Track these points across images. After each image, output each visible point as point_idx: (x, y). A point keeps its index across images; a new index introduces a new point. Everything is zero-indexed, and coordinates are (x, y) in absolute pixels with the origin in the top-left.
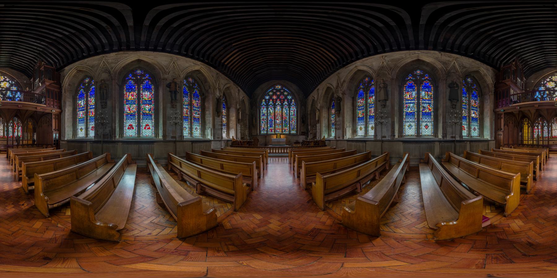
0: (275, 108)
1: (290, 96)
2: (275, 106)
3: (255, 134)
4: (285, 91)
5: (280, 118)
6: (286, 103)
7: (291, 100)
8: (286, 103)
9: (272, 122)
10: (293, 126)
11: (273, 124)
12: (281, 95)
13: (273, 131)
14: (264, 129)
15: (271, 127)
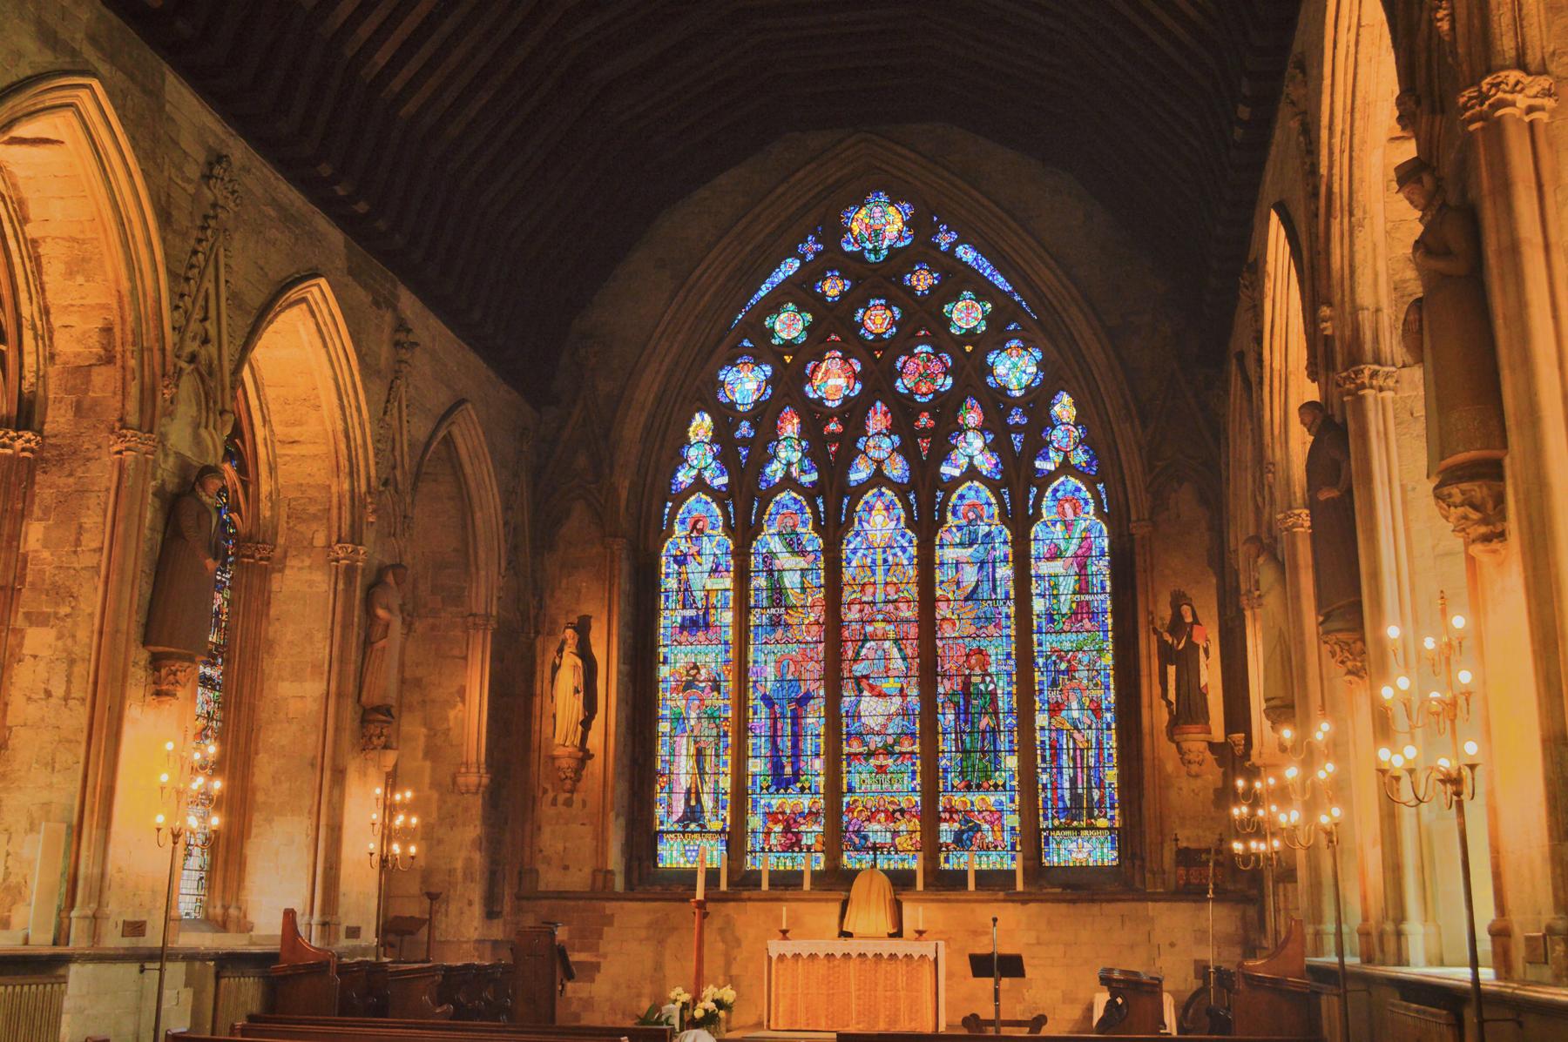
0: (834, 529)
1: (1027, 344)
2: (834, 510)
3: (577, 879)
4: (956, 280)
5: (898, 664)
6: (973, 449)
7: (1037, 401)
8: (973, 449)
9: (796, 719)
10: (1078, 755)
11: (808, 745)
12: (903, 341)
13: (812, 833)
14: (693, 814)
15: (781, 781)
